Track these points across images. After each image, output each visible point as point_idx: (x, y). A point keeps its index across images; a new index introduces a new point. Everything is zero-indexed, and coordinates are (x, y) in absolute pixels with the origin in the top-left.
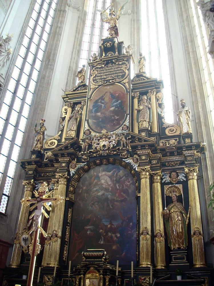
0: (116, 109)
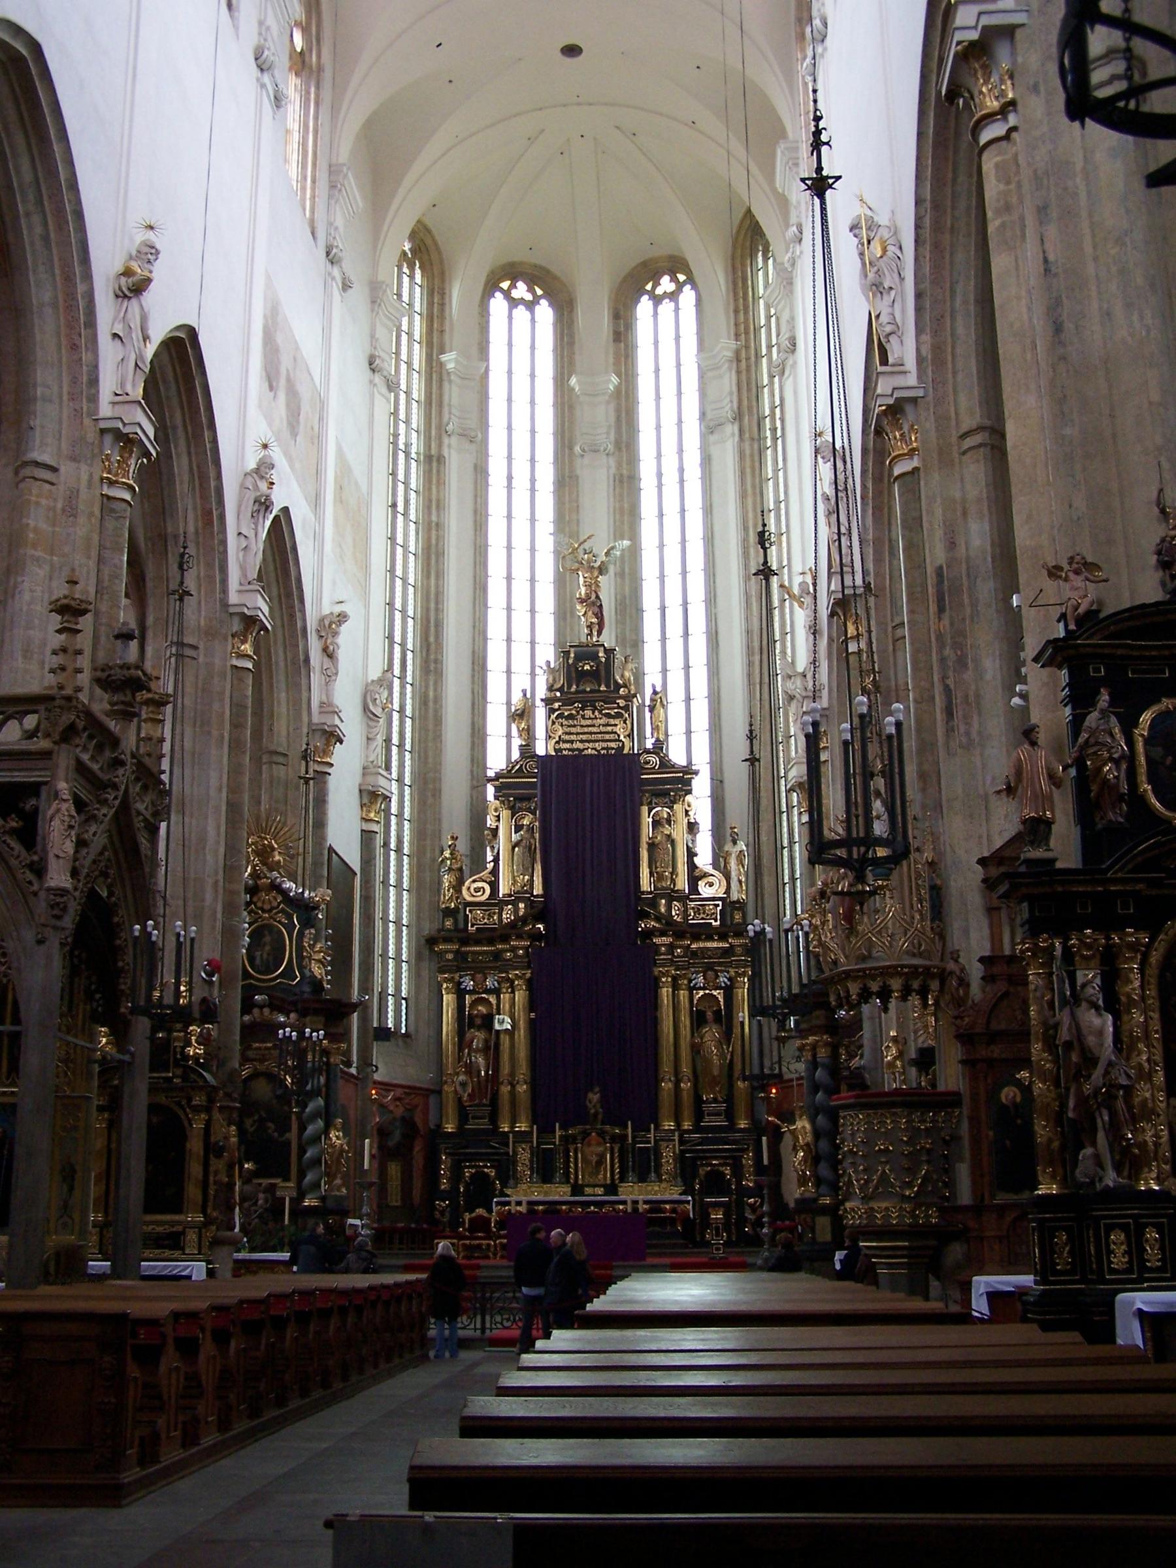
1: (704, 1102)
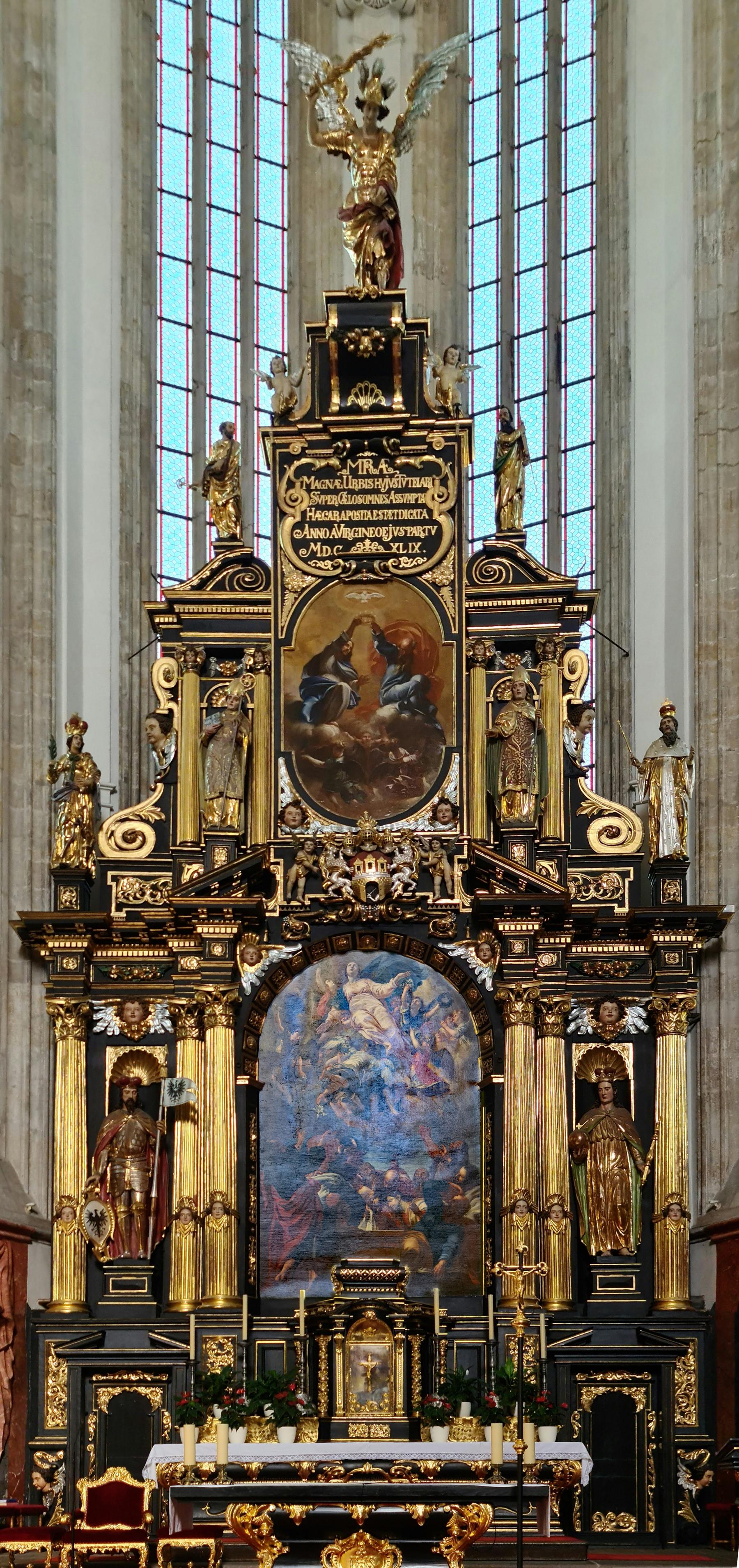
0: (405, 715)
1: (593, 1259)
